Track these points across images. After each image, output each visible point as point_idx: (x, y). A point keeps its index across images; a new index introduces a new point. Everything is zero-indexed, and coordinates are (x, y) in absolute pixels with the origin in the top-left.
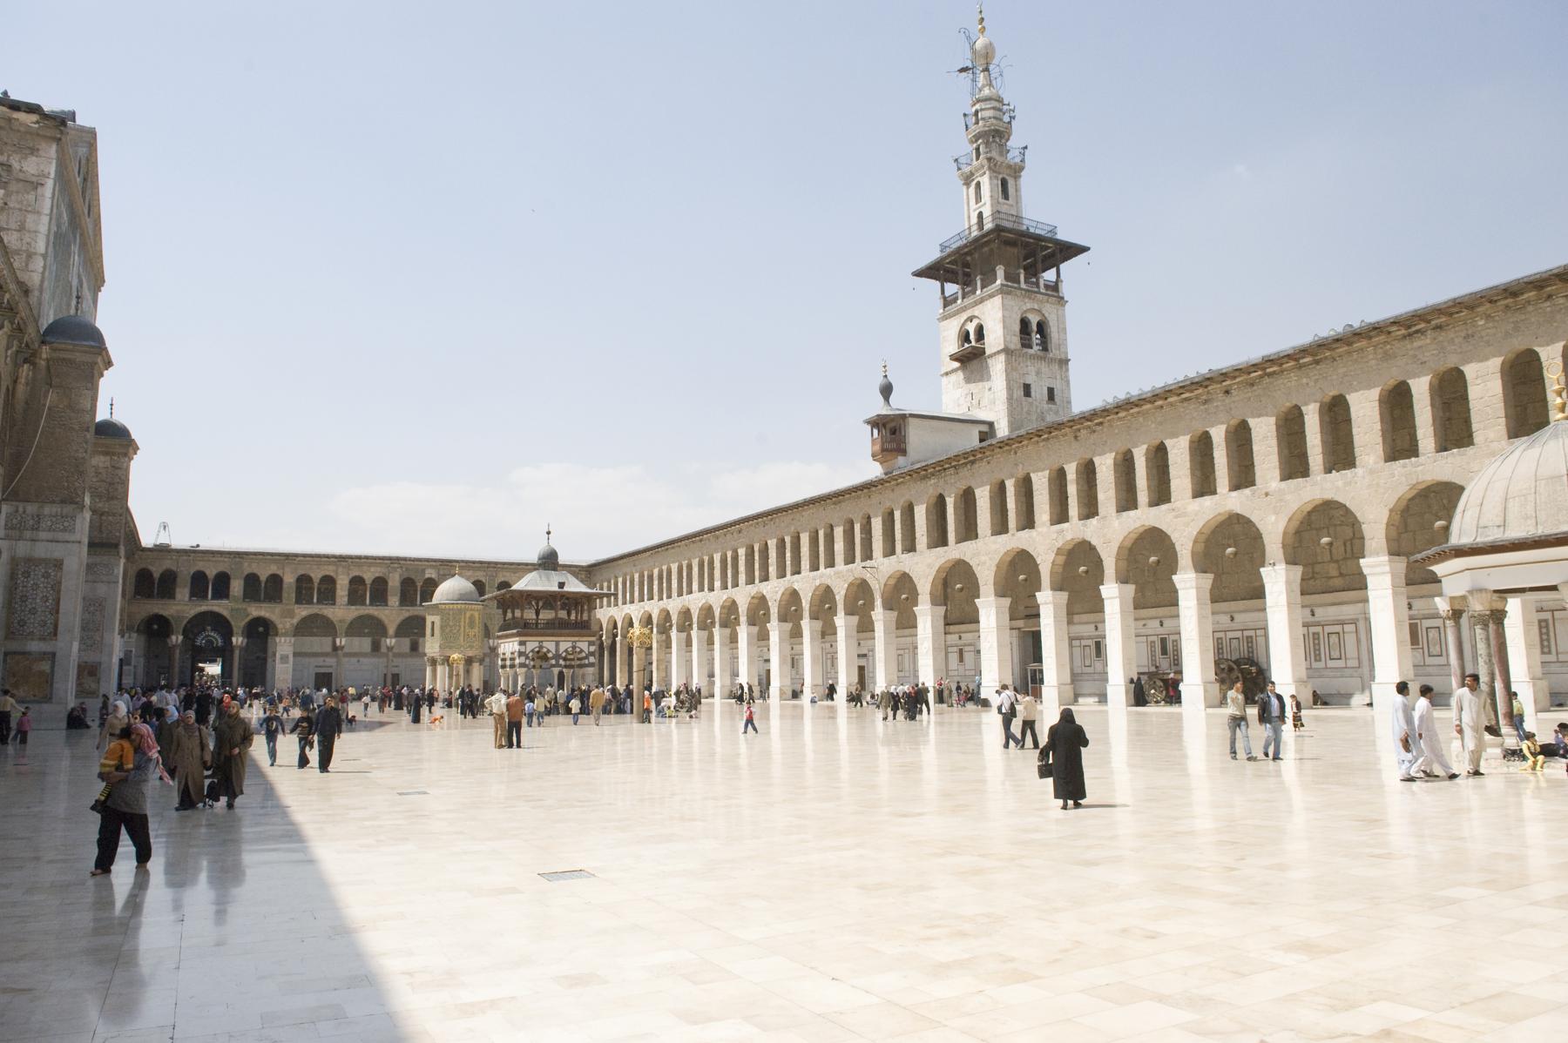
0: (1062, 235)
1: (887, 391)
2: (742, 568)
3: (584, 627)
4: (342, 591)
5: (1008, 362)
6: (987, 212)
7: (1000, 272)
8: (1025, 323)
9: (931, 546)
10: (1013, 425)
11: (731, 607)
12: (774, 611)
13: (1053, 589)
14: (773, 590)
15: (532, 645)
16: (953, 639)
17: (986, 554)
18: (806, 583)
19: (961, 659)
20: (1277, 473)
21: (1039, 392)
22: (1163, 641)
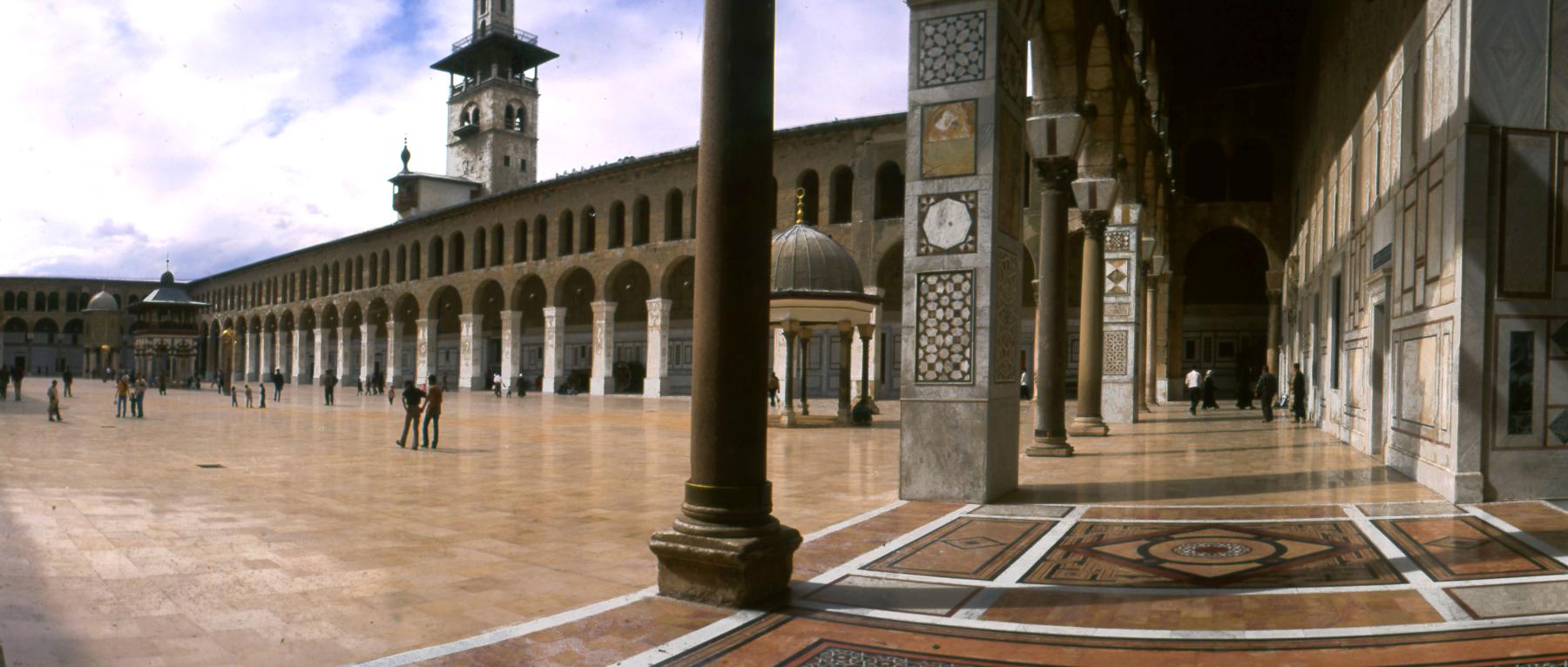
0: (540, 45)
1: (406, 156)
2: (297, 288)
3: (189, 328)
4: (31, 302)
5: (495, 139)
6: (488, 23)
7: (494, 71)
8: (509, 110)
9: (431, 275)
10: (494, 186)
11: (288, 316)
12: (319, 320)
13: (513, 309)
14: (318, 304)
15: (156, 341)
16: (443, 344)
17: (468, 281)
18: (340, 300)
19: (447, 358)
20: (662, 236)
21: (515, 161)
22: (583, 348)
